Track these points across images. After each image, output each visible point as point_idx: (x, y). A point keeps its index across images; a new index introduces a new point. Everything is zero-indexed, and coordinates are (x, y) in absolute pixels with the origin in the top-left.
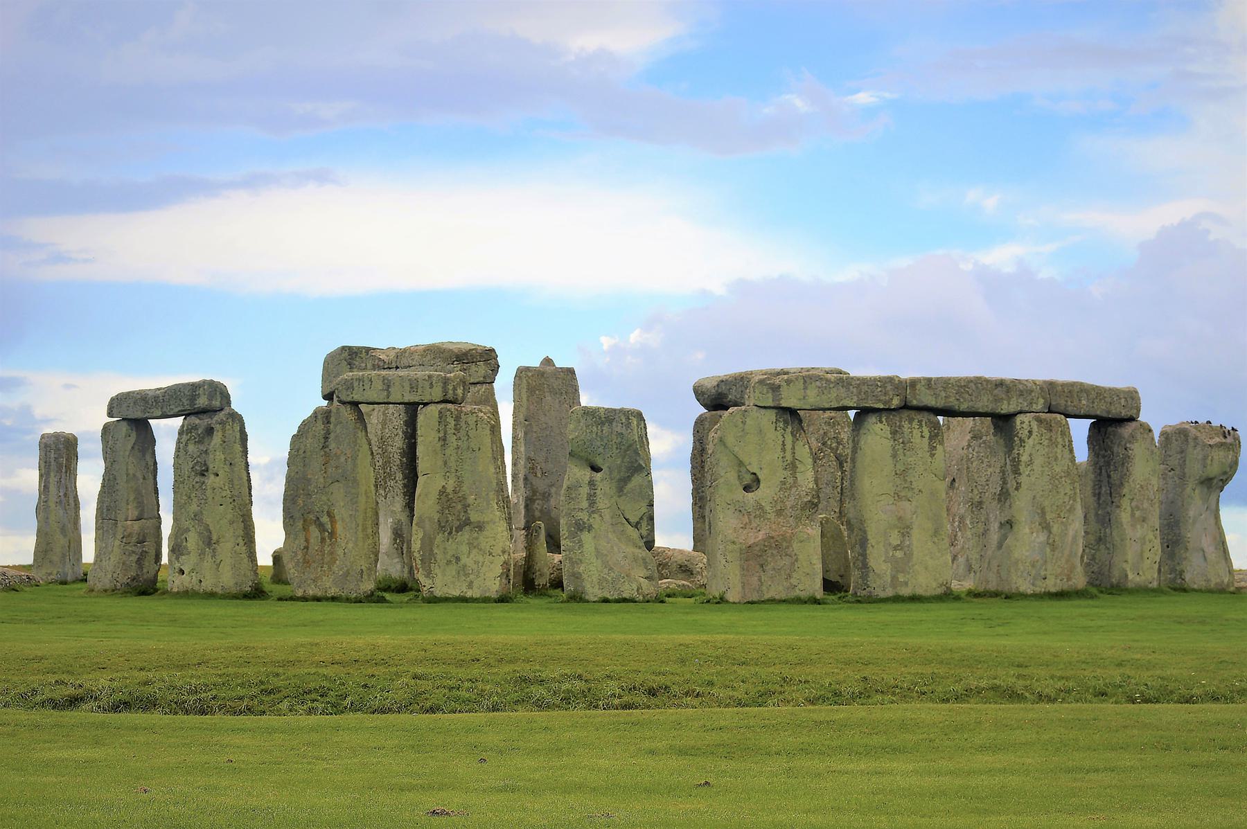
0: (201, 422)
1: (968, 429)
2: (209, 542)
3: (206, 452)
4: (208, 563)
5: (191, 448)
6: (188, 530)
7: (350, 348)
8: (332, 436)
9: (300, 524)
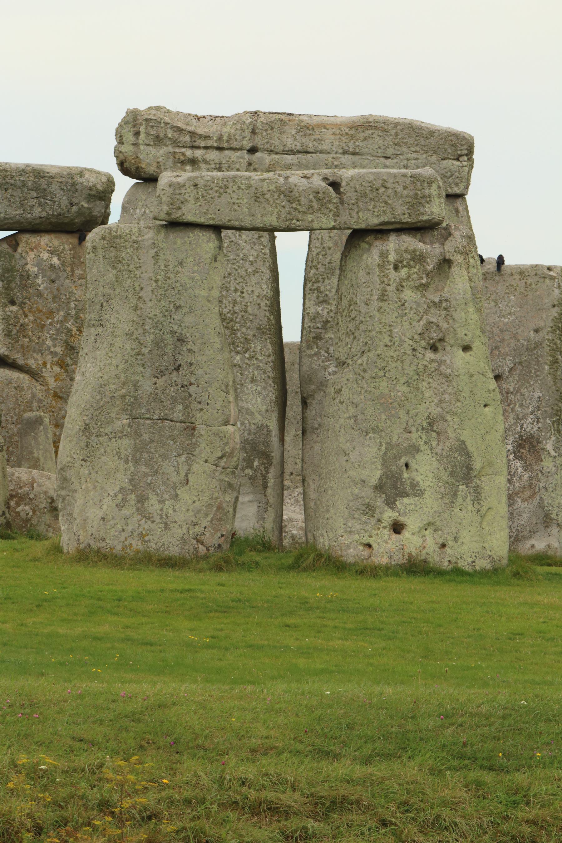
0: (431, 249)
1: (548, 302)
2: (462, 471)
3: (436, 305)
4: (465, 512)
5: (409, 295)
6: (415, 450)
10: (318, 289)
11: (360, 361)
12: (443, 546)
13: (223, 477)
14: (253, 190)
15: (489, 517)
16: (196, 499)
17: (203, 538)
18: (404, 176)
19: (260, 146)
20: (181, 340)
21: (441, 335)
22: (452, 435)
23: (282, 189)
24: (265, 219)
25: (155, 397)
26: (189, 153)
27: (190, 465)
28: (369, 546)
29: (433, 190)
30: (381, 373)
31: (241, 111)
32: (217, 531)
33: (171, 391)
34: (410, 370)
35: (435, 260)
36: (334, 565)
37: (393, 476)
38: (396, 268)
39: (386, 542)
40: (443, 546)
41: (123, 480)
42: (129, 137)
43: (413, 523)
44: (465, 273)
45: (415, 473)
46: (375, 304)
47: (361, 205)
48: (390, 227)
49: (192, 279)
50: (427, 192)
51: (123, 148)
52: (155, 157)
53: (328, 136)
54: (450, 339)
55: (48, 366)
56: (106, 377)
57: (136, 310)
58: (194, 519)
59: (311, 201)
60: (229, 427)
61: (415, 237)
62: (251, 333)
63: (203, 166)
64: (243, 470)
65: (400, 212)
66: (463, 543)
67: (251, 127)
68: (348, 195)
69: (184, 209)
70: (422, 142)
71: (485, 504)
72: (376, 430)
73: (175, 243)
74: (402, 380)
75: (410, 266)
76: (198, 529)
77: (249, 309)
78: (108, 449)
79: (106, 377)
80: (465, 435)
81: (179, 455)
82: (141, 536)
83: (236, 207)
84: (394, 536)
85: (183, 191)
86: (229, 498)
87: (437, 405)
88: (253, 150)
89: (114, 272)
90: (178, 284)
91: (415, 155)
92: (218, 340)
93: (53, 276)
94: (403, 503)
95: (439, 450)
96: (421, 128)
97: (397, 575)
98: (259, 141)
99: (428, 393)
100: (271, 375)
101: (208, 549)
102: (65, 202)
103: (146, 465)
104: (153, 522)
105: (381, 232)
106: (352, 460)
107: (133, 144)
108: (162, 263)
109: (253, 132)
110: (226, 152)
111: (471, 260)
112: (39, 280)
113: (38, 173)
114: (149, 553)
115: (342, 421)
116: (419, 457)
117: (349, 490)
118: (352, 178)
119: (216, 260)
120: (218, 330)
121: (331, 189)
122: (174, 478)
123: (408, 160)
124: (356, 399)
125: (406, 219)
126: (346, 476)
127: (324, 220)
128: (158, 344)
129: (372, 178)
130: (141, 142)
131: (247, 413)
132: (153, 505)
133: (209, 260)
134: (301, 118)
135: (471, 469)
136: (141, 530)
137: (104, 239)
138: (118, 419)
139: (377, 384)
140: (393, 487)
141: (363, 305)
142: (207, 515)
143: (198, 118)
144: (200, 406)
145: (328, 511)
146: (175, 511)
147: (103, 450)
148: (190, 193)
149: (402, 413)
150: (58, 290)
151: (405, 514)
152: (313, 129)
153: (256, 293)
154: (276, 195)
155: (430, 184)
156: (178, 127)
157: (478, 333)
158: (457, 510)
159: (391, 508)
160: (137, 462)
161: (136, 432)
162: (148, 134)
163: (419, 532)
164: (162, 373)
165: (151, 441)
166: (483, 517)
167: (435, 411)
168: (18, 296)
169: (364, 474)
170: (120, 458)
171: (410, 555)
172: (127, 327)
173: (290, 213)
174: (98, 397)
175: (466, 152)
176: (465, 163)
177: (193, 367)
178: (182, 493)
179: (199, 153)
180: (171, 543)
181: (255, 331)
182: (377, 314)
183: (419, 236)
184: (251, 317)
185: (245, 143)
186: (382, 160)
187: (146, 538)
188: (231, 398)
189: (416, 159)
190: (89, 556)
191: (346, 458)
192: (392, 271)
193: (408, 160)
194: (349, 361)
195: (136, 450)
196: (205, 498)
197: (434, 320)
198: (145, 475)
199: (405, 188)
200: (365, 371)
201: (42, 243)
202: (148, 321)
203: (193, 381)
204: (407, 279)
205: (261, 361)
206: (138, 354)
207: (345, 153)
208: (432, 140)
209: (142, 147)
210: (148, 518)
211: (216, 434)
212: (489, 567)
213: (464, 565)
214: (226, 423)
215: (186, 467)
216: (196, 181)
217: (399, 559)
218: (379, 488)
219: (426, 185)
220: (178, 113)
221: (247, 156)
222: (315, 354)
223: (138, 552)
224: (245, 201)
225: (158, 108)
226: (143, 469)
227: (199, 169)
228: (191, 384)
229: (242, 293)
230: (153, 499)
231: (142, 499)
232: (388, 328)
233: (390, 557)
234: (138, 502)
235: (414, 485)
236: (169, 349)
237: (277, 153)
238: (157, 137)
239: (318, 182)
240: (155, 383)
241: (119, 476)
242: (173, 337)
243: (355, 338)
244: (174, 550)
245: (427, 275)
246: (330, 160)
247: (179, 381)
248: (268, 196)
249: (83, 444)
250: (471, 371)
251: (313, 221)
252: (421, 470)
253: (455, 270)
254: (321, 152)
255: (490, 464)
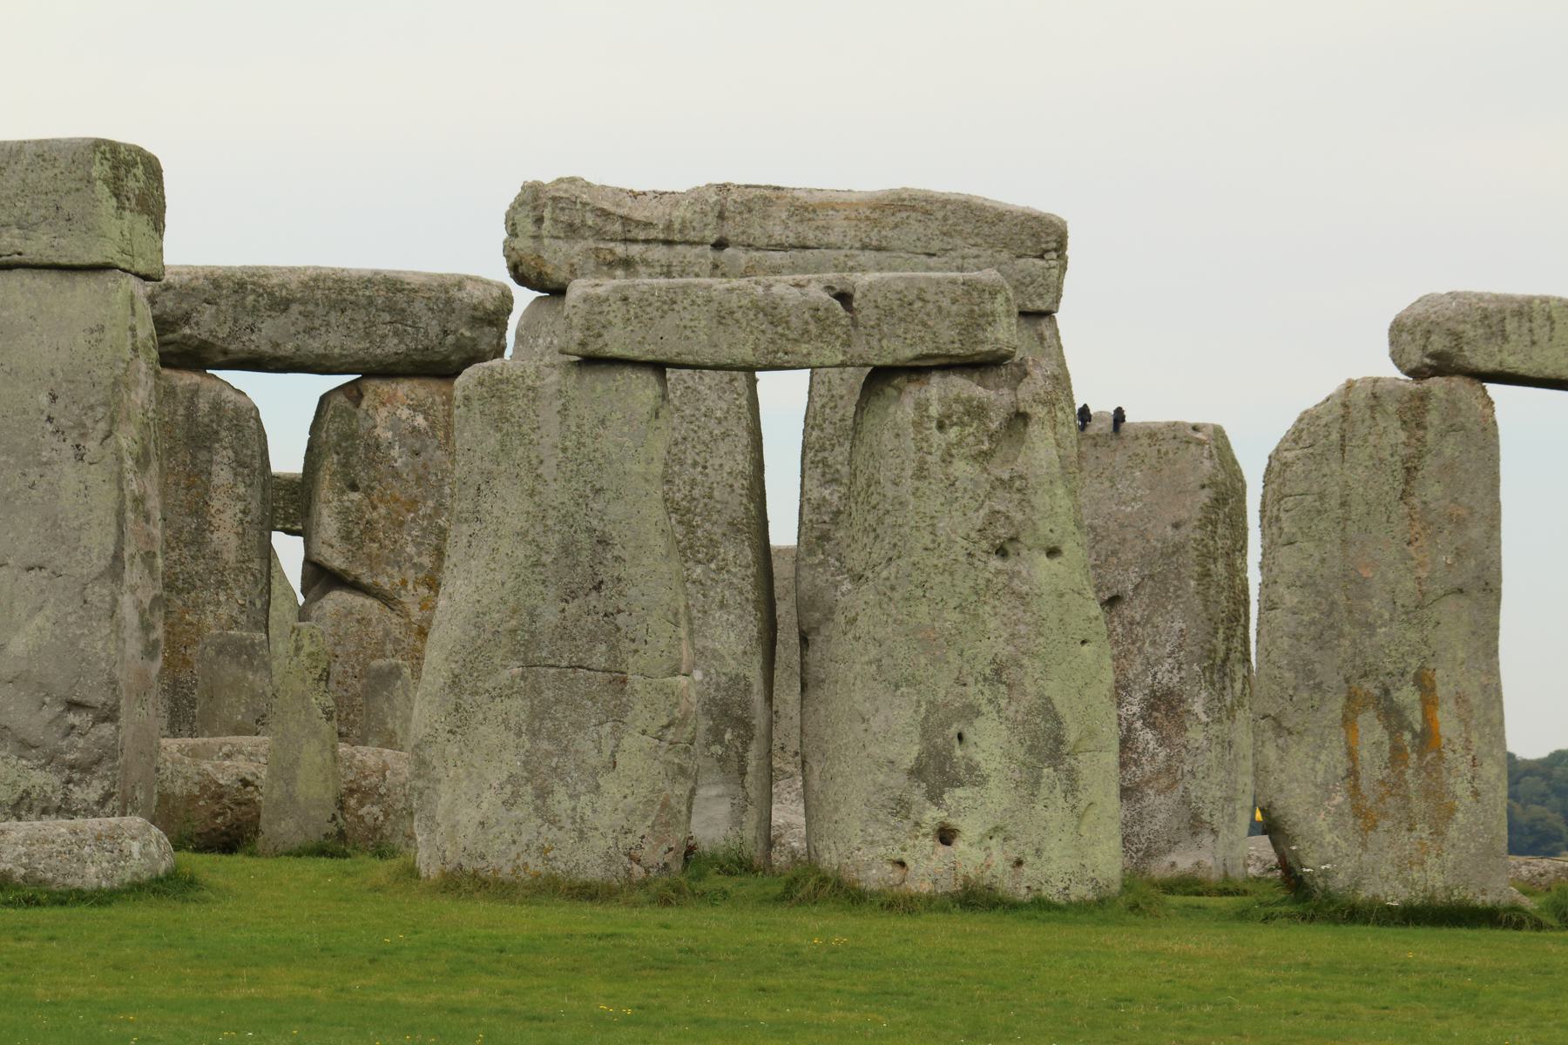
1: (1193, 480)
2: (1048, 746)
3: (1005, 484)
5: (962, 469)
7: (114, 147)
8: (1430, 464)
9: (1337, 705)
10: (824, 461)
11: (885, 574)
12: (1019, 863)
13: (670, 757)
14: (715, 305)
15: (1091, 817)
16: (628, 791)
17: (639, 853)
18: (953, 282)
19: (731, 238)
20: (603, 542)
21: (1012, 532)
22: (1031, 689)
23: (761, 304)
24: (734, 351)
25: (563, 633)
26: (620, 249)
27: (619, 739)
28: (902, 864)
29: (999, 305)
30: (919, 592)
31: (702, 184)
32: (662, 842)
33: (588, 622)
34: (964, 587)
35: (1003, 414)
36: (845, 894)
37: (939, 754)
38: (941, 427)
39: (929, 859)
40: (1019, 863)
41: (512, 763)
42: (528, 226)
43: (970, 828)
44: (1051, 434)
45: (972, 749)
46: (908, 484)
47: (885, 328)
48: (931, 363)
49: (621, 446)
50: (988, 307)
51: (517, 244)
52: (567, 256)
53: (839, 222)
54: (1027, 538)
55: (410, 586)
56: (485, 601)
57: (531, 496)
58: (624, 823)
59: (807, 323)
60: (680, 678)
61: (970, 377)
62: (720, 531)
63: (642, 269)
64: (707, 746)
65: (946, 339)
66: (1049, 859)
67: (718, 208)
68: (865, 312)
69: (606, 337)
70: (986, 230)
71: (1084, 798)
72: (911, 681)
73: (594, 390)
74: (953, 602)
75: (962, 424)
76: (631, 840)
77: (716, 494)
78: (490, 715)
79: (485, 601)
80: (1052, 689)
81: (601, 724)
82: (543, 850)
83: (688, 332)
84: (941, 849)
85: (605, 308)
86: (681, 790)
87: (1007, 642)
88: (720, 245)
89: (498, 435)
90: (598, 455)
91: (974, 251)
92: (661, 541)
93: (417, 446)
94: (953, 796)
95: (1010, 713)
96: (983, 209)
97: (945, 910)
98: (730, 230)
99: (992, 624)
100: (751, 596)
101: (647, 872)
102: (434, 329)
103: (550, 738)
104: (561, 828)
105: (917, 370)
106: (875, 729)
107: (534, 237)
108: (572, 422)
109: (721, 216)
110: (679, 248)
111: (1060, 414)
112: (395, 452)
113: (394, 285)
114: (555, 878)
115: (858, 667)
116: (978, 723)
117: (870, 777)
118: (871, 286)
119: (657, 417)
120: (661, 526)
121: (837, 304)
122: (593, 759)
123: (963, 258)
124: (880, 633)
125: (956, 349)
126: (864, 754)
127: (827, 352)
128: (565, 549)
129: (902, 286)
130: (544, 233)
131: (714, 657)
132: (561, 802)
133: (646, 417)
134: (796, 193)
135: (1062, 742)
136: (541, 841)
137: (481, 384)
138: (505, 667)
139: (912, 610)
140: (938, 771)
141: (889, 485)
142: (645, 817)
143: (635, 195)
144: (633, 646)
145: (836, 809)
146: (594, 811)
147: (481, 716)
148: (616, 312)
149: (952, 655)
150: (425, 466)
151: (958, 814)
152: (814, 211)
153: (727, 469)
154: (751, 314)
155: (993, 294)
156: (603, 210)
157: (1071, 527)
158: (1039, 807)
159: (936, 804)
160: (535, 735)
161: (533, 687)
162: (555, 221)
163: (981, 842)
164: (573, 595)
165: (557, 702)
166: (1080, 817)
167: (1005, 651)
168: (363, 477)
169: (893, 750)
170: (508, 728)
171: (966, 878)
172: (518, 523)
173: (773, 342)
174: (474, 633)
175: (1054, 245)
176: (1053, 263)
177: (622, 584)
178: (608, 783)
179: (635, 250)
180: (589, 862)
181: (724, 529)
182: (912, 499)
183: (976, 376)
184: (719, 506)
185: (707, 233)
186: (924, 258)
187: (551, 855)
188: (683, 633)
189: (977, 257)
190: (461, 883)
191: (864, 726)
192: (935, 431)
193: (963, 258)
194: (869, 574)
195: (533, 715)
196: (642, 791)
197: (1003, 509)
198: (548, 754)
199: (954, 301)
200: (893, 588)
201: (400, 394)
202: (551, 512)
203: (622, 606)
204: (959, 444)
205: (735, 575)
206: (535, 565)
207: (864, 247)
208: (1001, 227)
209: (546, 241)
210: (553, 823)
211: (659, 690)
212: (1091, 896)
213: (1051, 893)
214: (675, 672)
215: (612, 742)
216: (626, 293)
217: (949, 885)
218: (916, 773)
219: (987, 296)
220: (604, 187)
221: (711, 254)
222: (821, 564)
223: (538, 875)
224: (703, 323)
225: (572, 180)
226: (545, 745)
227: (636, 274)
228: (619, 612)
229: (705, 467)
230: (561, 793)
231: (543, 793)
232: (928, 521)
233: (935, 882)
234: (538, 797)
235: (972, 768)
236: (584, 557)
237: (758, 249)
238: (571, 225)
239: (816, 293)
240: (563, 611)
241: (507, 756)
242: (590, 537)
243: (877, 537)
244: (595, 873)
245: (991, 437)
246: (842, 258)
247: (600, 607)
248: (738, 315)
249: (450, 707)
250: (1061, 587)
251: (809, 354)
252: (984, 745)
253: (1034, 429)
254: (828, 247)
255: (1092, 734)
